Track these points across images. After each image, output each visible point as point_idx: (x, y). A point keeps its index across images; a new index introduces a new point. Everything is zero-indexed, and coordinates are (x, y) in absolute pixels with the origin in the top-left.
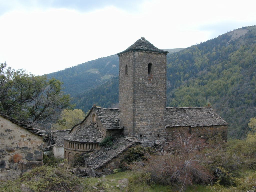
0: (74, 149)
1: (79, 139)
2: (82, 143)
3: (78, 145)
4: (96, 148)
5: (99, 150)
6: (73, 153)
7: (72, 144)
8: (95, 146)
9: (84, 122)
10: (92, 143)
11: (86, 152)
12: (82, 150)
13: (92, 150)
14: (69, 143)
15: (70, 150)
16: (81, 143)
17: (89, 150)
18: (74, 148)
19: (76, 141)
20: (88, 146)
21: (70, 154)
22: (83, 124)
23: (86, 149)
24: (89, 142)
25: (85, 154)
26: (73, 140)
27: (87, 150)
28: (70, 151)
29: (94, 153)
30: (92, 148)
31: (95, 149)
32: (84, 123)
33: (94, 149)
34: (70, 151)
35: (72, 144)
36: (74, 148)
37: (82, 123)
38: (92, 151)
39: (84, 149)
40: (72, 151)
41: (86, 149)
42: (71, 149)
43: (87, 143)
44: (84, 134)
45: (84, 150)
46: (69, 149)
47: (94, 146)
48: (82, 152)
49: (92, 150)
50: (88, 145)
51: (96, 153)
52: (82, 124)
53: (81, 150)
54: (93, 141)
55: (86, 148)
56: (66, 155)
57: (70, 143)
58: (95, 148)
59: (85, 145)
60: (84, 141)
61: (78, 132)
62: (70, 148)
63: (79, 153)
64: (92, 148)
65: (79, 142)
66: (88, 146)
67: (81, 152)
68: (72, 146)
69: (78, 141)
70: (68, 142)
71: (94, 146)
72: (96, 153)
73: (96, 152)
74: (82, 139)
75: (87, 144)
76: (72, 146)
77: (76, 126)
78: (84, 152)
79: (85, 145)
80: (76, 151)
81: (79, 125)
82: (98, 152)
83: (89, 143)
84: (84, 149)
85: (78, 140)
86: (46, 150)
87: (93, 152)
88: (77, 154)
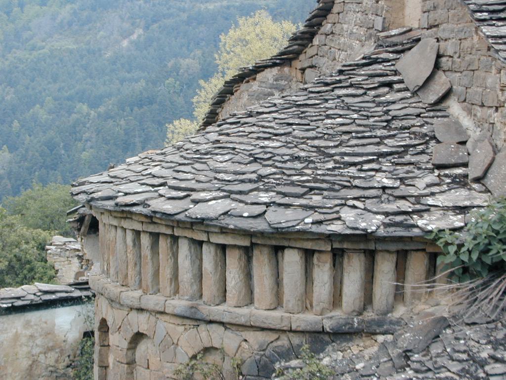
0: (179, 304)
1: (229, 194)
2: (262, 234)
3: (249, 259)
4: (416, 297)
5: (443, 323)
6: (169, 345)
7: (163, 244)
8: (400, 271)
9: (316, 41)
10: (366, 236)
11: (296, 340)
12: (259, 312)
13: (369, 315)
14: (137, 233)
15: (140, 310)
16: (246, 243)
17: (337, 313)
18: (176, 291)
19: (198, 211)
20: (322, 273)
21: (143, 347)
22: (303, 61)
23: (306, 304)
24: (336, 227)
25: (294, 363)
26: (169, 207)
27: (307, 320)
28: (143, 317)
29: (384, 345)
30: (368, 299)
31: (400, 311)
32: (310, 51)
33: (391, 309)
34: (142, 322)
35: (163, 244)
36: (176, 291)
37: (297, 54)
38: (367, 332)
39: (278, 302)
40: (164, 326)
41: (306, 304)
42: (152, 301)
43: (303, 234)
44: (286, 145)
45: (275, 317)
46: (132, 296)
47: (385, 267)
48: (255, 339)
49: (369, 315)
50: (328, 258)
51: (406, 355)
52: (297, 64)
53: (244, 314)
54: (373, 223)
55: (301, 289)
56: (111, 360)
57: (145, 240)
58: (399, 295)
59: (292, 260)
60: (280, 218)
61: (234, 129)
62: (138, 293)
63: (229, 340)
64: (368, 299)
65: (224, 231)
66: (322, 273)
67: (251, 336)
68: (166, 272)
69: (212, 214)
70: (126, 224)
71: (385, 267)
72: (406, 355)
73: (407, 338)
74: (264, 197)
75: (309, 245)
76: (166, 272)
77: (243, 86)
78: (284, 342)
79: (292, 260)
80: (193, 319)
81: (270, 74)
82: (436, 349)
83: (330, 237)
84: (278, 302)
85: (214, 208)
86: (77, 294)
87: (381, 338)
88: (207, 350)
